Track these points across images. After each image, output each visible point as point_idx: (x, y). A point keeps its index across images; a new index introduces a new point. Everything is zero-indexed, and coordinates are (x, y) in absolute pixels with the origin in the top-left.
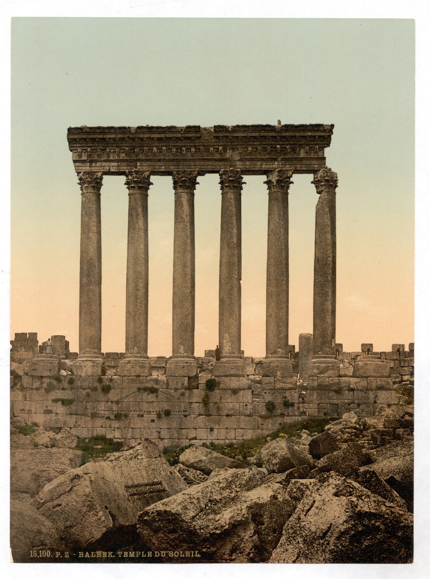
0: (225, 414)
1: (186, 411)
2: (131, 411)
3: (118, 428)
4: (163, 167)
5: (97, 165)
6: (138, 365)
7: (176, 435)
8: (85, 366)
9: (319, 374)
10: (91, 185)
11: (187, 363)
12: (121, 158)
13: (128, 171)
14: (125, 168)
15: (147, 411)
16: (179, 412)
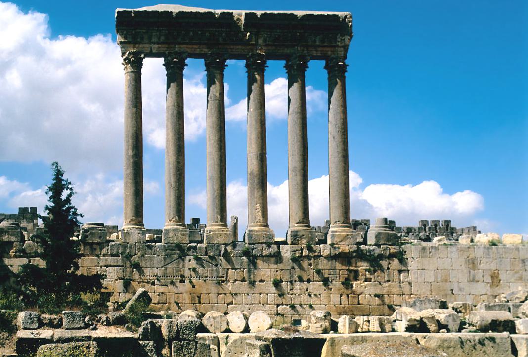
0: (258, 280)
1: (224, 277)
2: (174, 277)
3: (162, 293)
4: (198, 50)
5: (140, 46)
6: (180, 233)
7: (215, 300)
8: (132, 233)
9: (340, 242)
10: (135, 64)
11: (223, 231)
12: (162, 40)
13: (168, 53)
14: (165, 49)
15: (189, 277)
16: (217, 277)
